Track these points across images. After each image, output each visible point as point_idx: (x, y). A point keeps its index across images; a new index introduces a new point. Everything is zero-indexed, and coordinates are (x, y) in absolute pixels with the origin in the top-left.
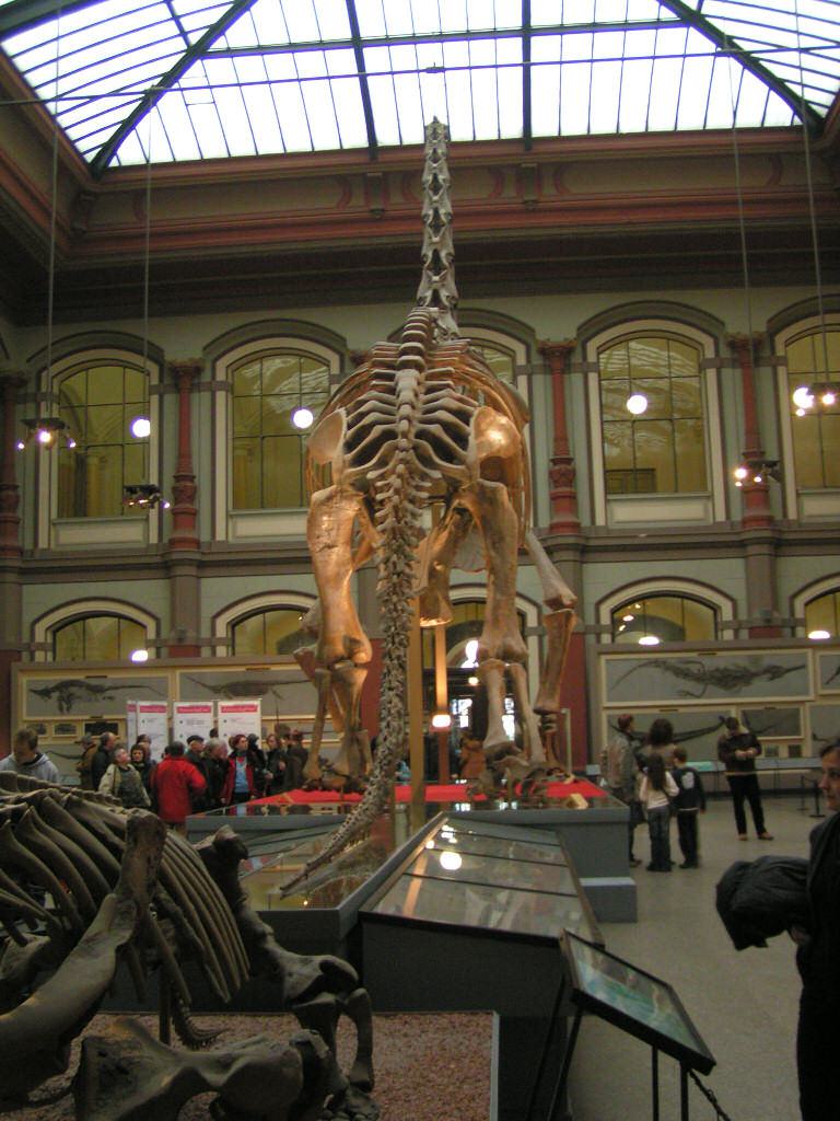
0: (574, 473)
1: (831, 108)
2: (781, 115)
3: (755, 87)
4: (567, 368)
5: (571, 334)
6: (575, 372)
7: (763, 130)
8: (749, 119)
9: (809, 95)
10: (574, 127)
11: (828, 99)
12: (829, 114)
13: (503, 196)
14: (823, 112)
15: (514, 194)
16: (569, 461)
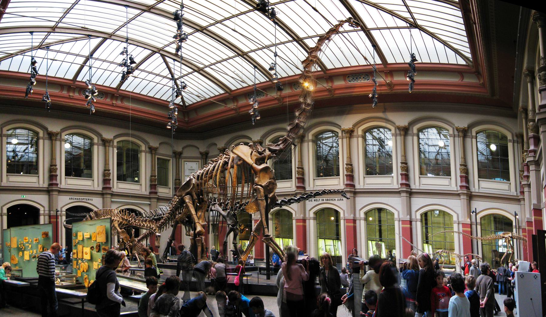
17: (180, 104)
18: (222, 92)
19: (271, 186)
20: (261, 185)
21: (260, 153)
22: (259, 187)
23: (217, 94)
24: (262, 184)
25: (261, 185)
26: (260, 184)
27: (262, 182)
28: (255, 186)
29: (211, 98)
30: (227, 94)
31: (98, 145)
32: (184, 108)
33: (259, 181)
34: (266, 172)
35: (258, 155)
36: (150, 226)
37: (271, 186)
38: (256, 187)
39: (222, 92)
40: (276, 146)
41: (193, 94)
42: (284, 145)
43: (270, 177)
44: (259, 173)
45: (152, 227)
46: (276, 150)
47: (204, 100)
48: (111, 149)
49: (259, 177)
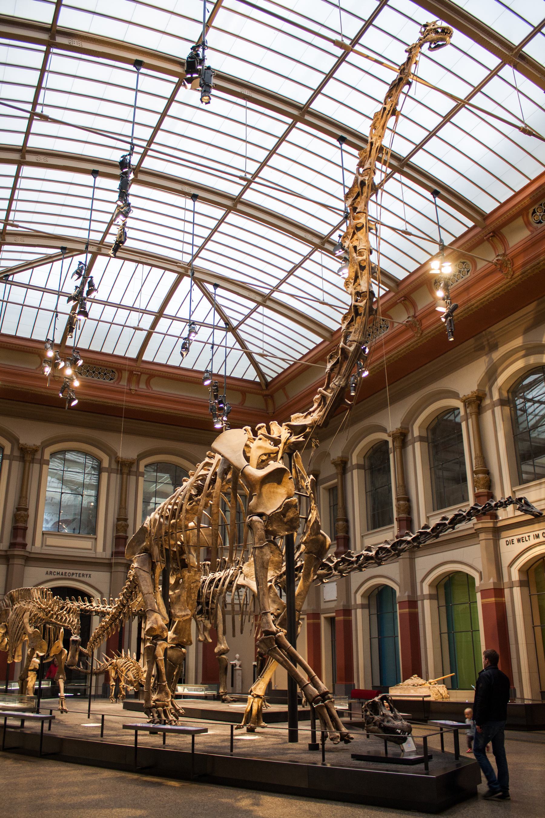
0: (127, 526)
1: (274, 379)
2: (252, 375)
3: (245, 361)
4: (129, 473)
5: (135, 457)
6: (133, 475)
7: (242, 380)
8: (237, 374)
9: (264, 370)
10: (161, 359)
11: (274, 375)
12: (271, 381)
13: (121, 383)
14: (269, 379)
15: (126, 384)
16: (126, 520)
17: (256, 380)
18: (319, 340)
19: (291, 514)
20: (261, 515)
21: (276, 442)
22: (255, 518)
23: (312, 346)
24: (268, 510)
25: (261, 515)
26: (260, 510)
27: (266, 507)
28: (250, 517)
29: (304, 356)
30: (327, 343)
31: (110, 471)
32: (264, 387)
33: (257, 505)
34: (279, 482)
35: (269, 446)
36: (73, 621)
37: (291, 514)
38: (251, 519)
39: (319, 340)
40: (305, 417)
41: (275, 356)
42: (320, 411)
43: (288, 493)
44: (258, 487)
45: (73, 623)
46: (304, 427)
47: (293, 364)
48: (133, 478)
49: (260, 496)
